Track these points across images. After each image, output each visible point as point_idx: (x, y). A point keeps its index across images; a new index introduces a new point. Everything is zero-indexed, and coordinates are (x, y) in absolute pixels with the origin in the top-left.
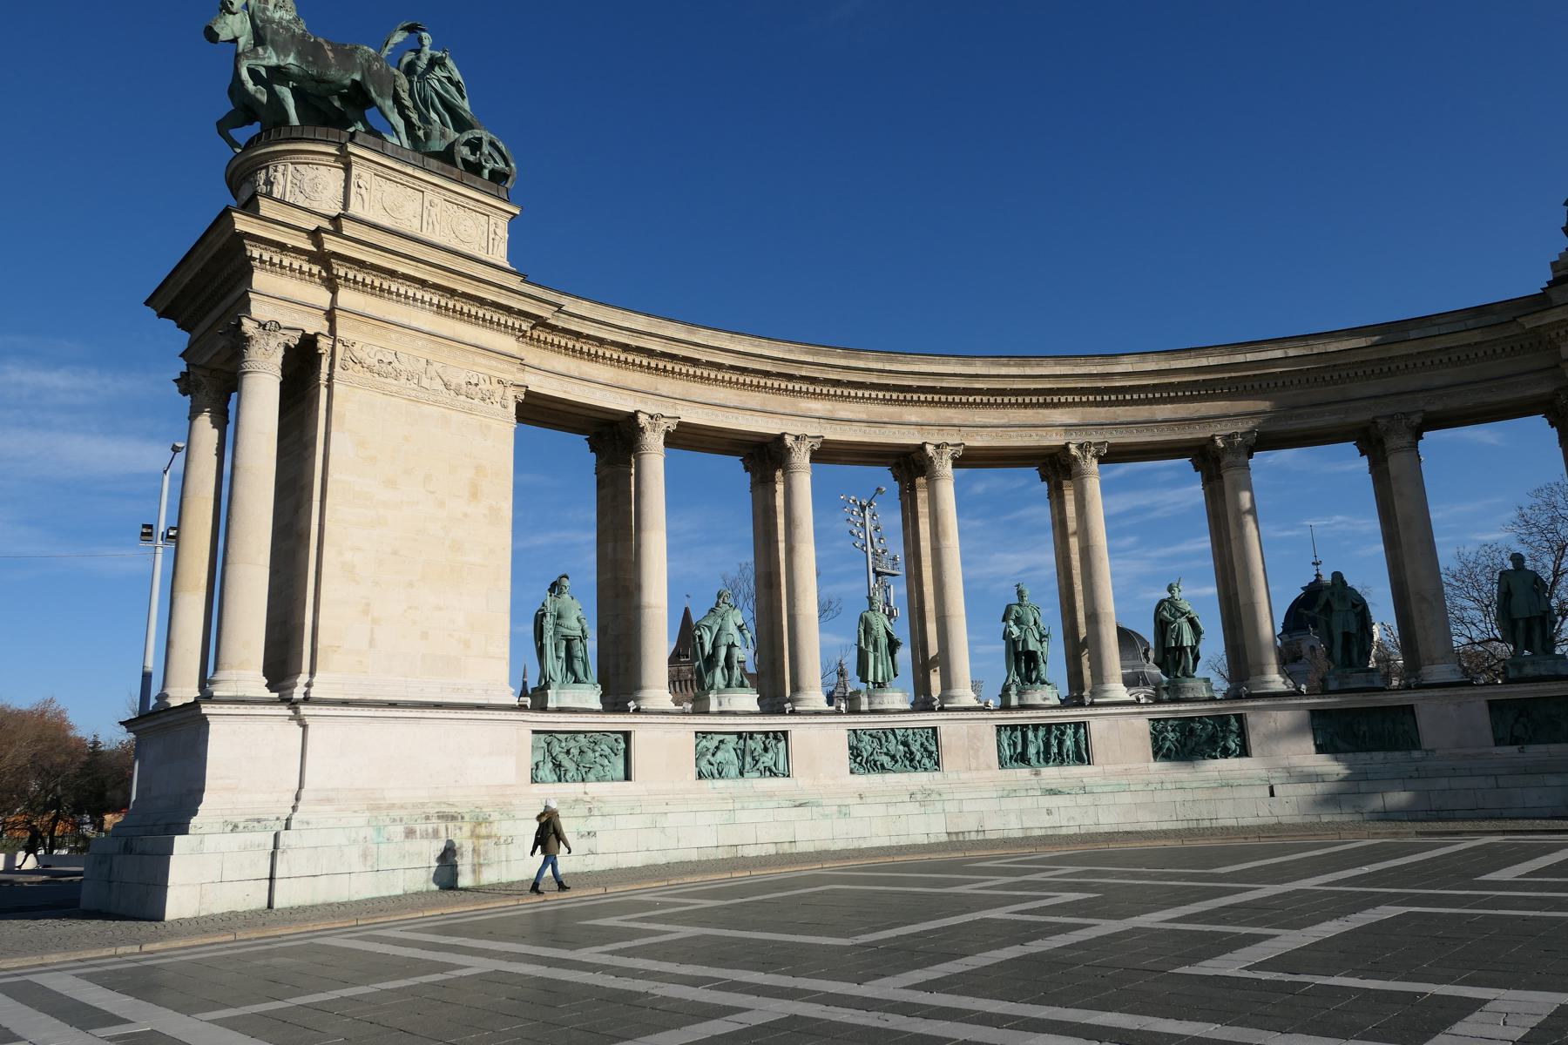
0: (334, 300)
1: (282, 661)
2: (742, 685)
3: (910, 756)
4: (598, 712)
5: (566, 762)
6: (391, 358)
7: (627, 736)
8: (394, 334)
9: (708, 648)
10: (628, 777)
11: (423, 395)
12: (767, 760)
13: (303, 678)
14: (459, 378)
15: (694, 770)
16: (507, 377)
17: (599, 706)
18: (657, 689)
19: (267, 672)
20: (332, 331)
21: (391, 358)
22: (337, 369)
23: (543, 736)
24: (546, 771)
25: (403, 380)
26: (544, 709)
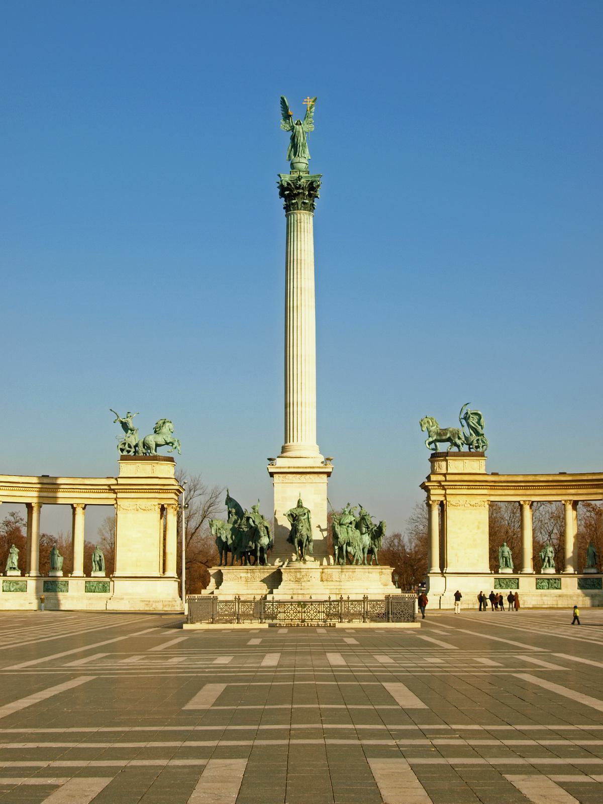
0: (446, 492)
1: (443, 564)
2: (552, 567)
3: (594, 585)
4: (511, 574)
5: (502, 584)
6: (458, 502)
7: (518, 579)
8: (458, 496)
9: (543, 557)
10: (518, 588)
11: (465, 508)
12: (556, 585)
13: (445, 569)
14: (472, 503)
15: (535, 587)
16: (484, 500)
17: (512, 572)
18: (528, 567)
19: (440, 567)
20: (446, 499)
21: (458, 502)
22: (447, 507)
23: (498, 580)
24: (498, 586)
25: (461, 506)
26: (499, 574)
